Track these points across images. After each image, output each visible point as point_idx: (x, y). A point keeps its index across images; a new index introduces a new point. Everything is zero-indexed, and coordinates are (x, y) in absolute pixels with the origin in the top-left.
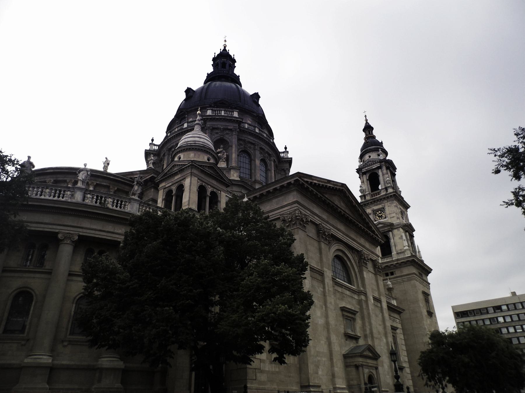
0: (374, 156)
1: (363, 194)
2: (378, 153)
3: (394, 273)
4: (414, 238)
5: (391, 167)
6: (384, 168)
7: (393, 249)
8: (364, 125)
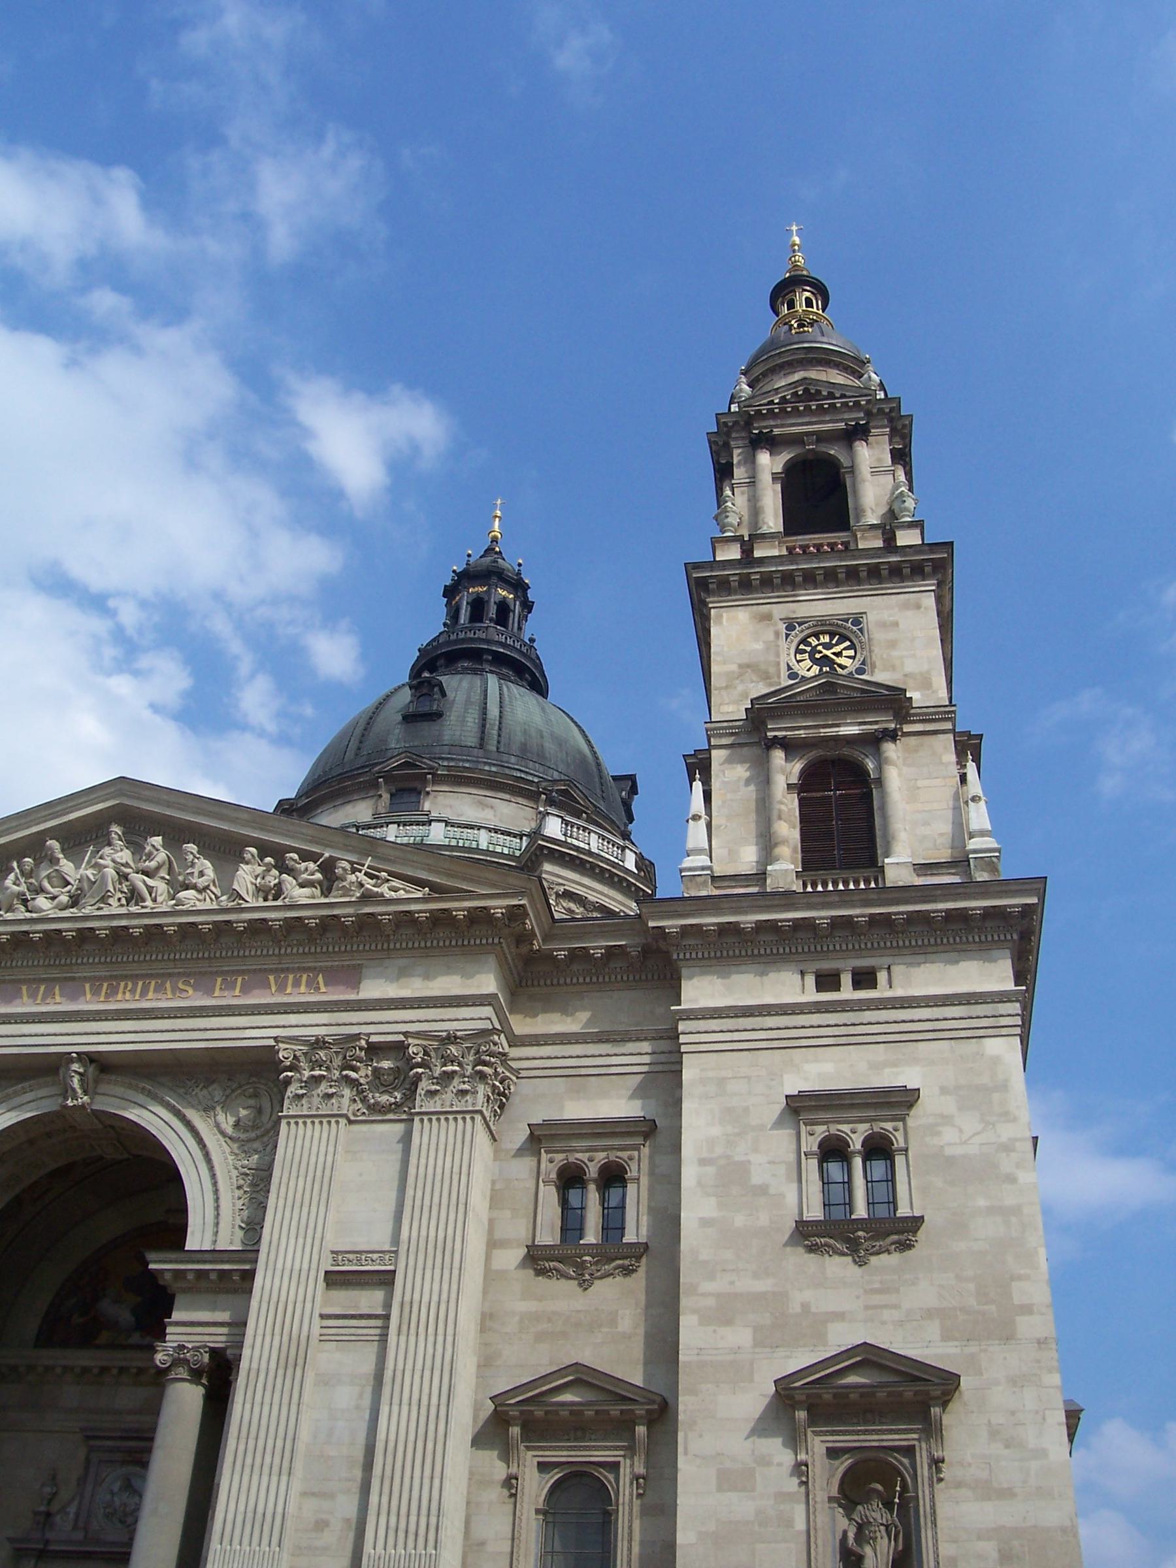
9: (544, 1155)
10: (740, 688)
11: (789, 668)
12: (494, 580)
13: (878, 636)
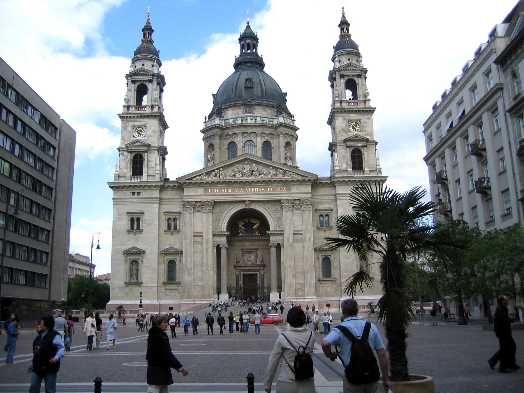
0: (148, 65)
1: (127, 105)
2: (153, 63)
3: (141, 193)
4: (165, 161)
5: (161, 82)
6: (155, 82)
7: (145, 170)
8: (145, 24)
9: (318, 213)
10: (341, 134)
11: (349, 130)
12: (252, 38)
13: (364, 125)
